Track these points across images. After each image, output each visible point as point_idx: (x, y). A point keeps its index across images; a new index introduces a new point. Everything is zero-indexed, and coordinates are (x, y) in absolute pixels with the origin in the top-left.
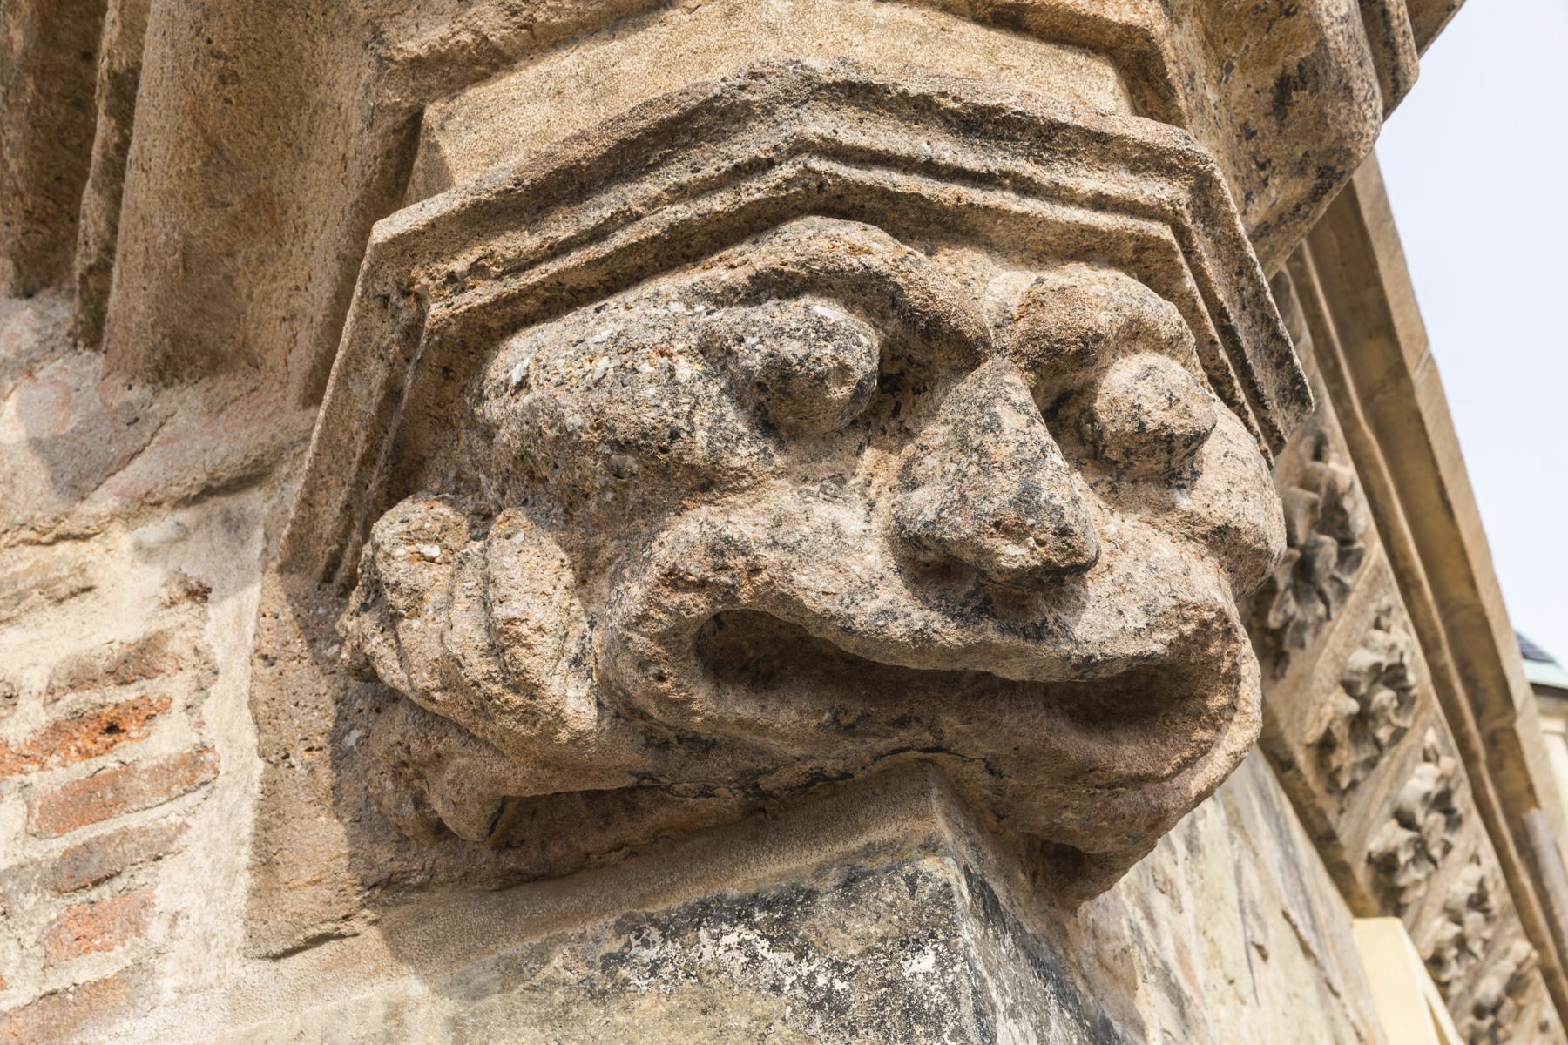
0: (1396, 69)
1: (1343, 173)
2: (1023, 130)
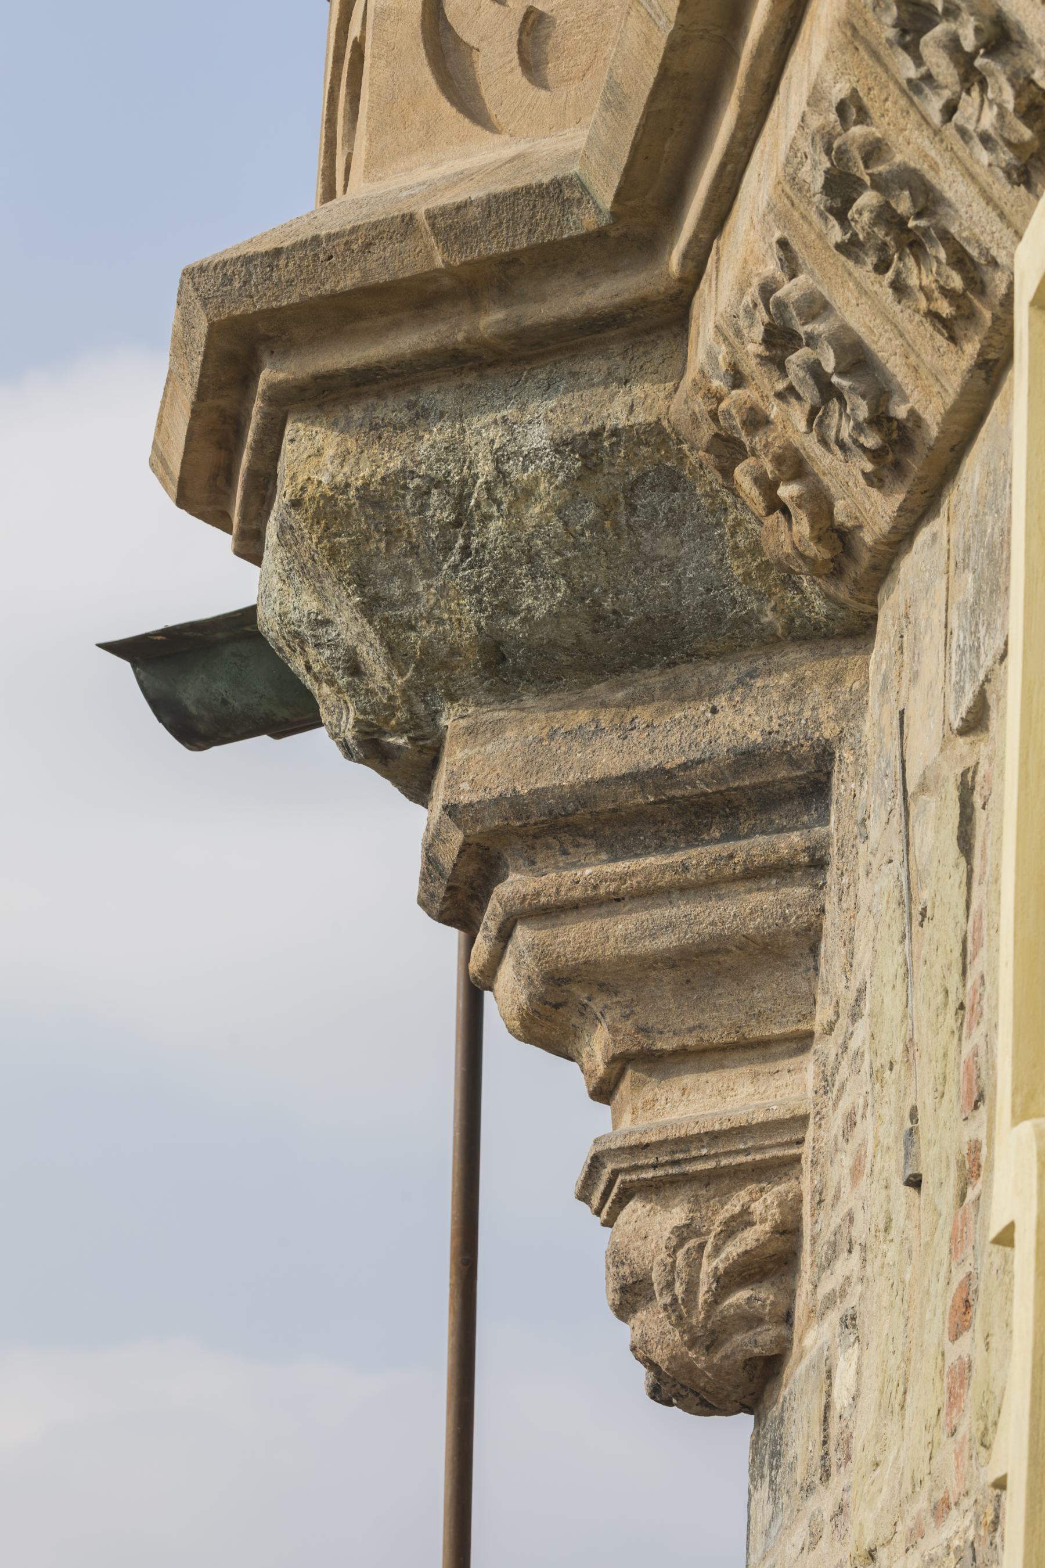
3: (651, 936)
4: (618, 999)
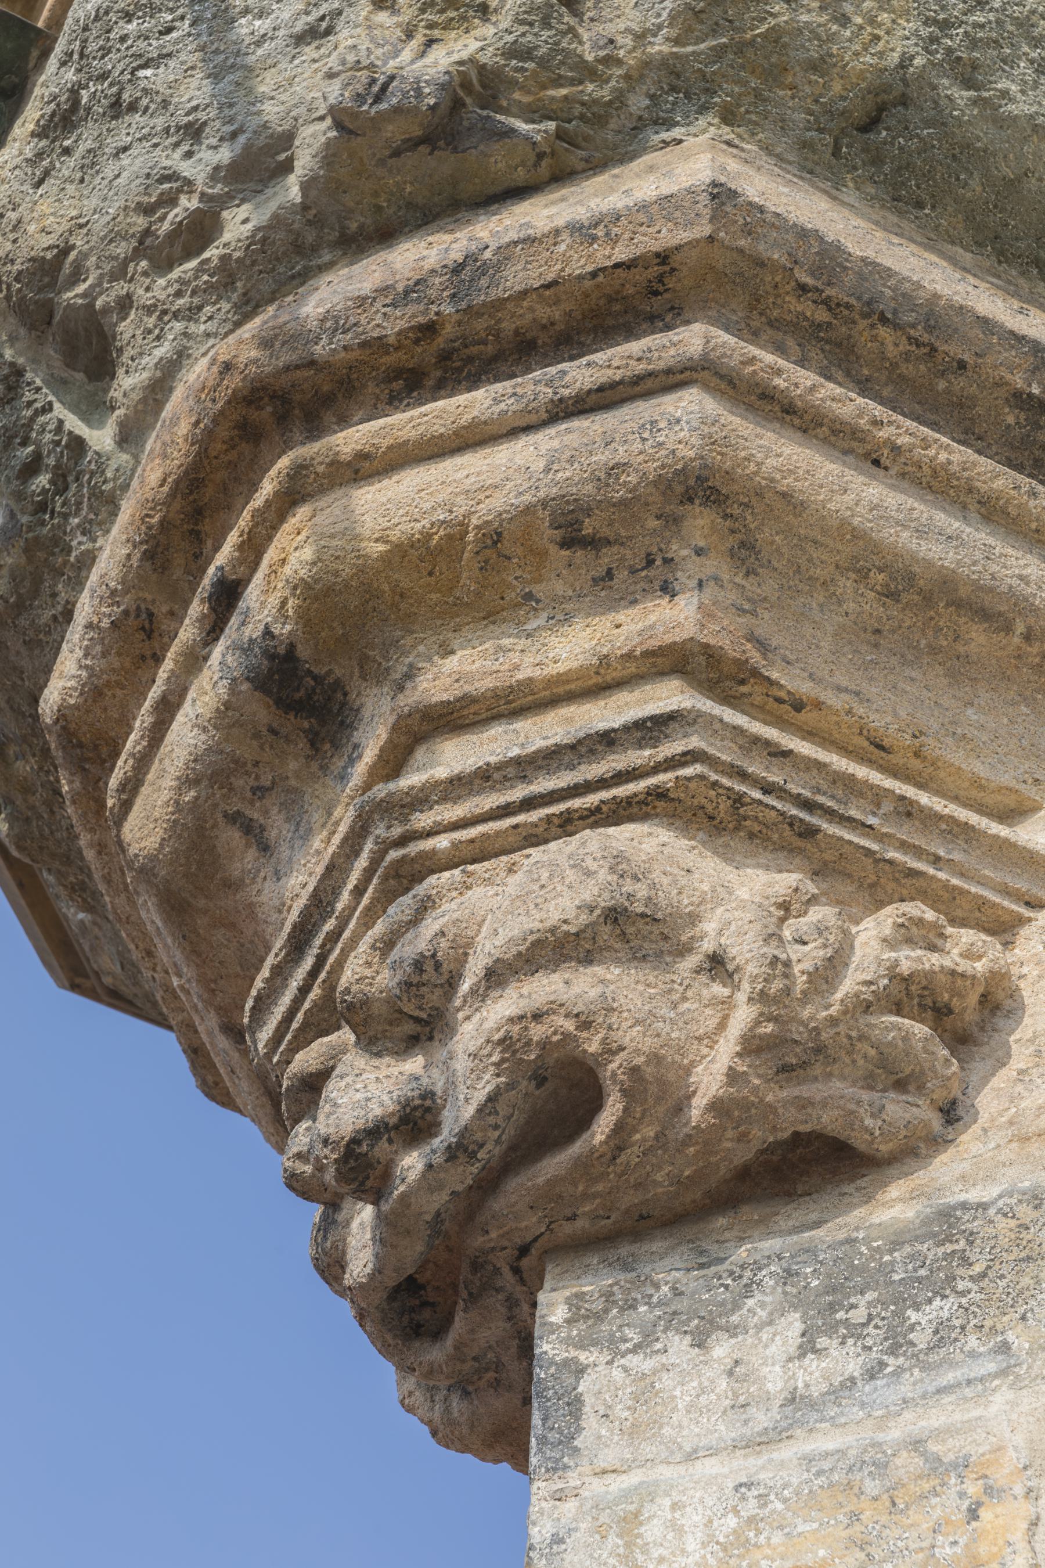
0: (669, 371)
1: (698, 478)
2: (311, 915)
3: (918, 531)
4: (744, 582)
